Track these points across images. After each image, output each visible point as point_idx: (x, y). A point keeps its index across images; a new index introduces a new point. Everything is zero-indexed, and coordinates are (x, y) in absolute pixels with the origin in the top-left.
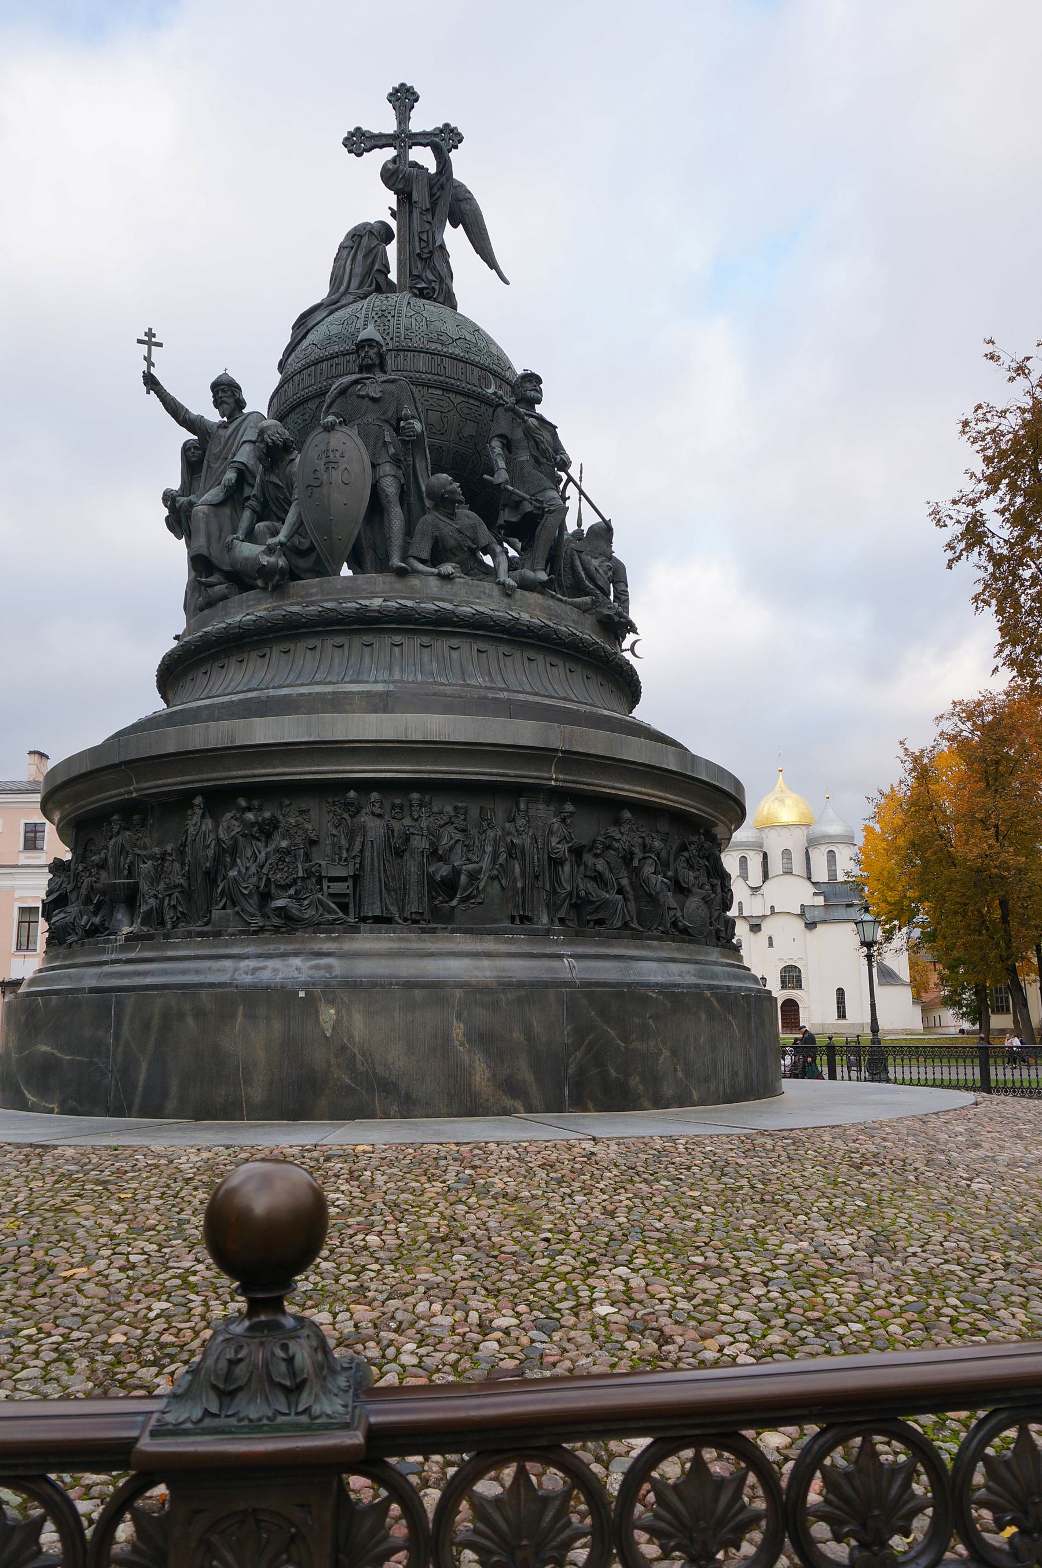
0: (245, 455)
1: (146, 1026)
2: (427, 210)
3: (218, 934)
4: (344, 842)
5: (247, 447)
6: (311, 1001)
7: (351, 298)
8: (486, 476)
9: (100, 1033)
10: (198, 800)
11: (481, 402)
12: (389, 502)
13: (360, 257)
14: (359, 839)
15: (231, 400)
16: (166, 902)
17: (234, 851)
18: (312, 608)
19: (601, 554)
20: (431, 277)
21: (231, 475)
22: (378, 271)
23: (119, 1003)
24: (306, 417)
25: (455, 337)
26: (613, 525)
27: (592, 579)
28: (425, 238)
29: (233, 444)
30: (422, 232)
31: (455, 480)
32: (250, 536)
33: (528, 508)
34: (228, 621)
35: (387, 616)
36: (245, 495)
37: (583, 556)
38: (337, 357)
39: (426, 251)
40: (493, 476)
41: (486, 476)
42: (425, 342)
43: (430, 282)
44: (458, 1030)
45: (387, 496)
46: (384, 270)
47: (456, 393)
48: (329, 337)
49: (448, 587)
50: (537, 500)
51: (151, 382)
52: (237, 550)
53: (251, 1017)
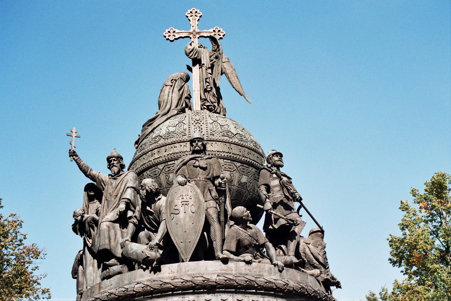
0: (129, 194)
2: (209, 68)
7: (176, 112)
8: (258, 205)
11: (249, 166)
12: (214, 221)
13: (176, 90)
15: (118, 165)
18: (177, 280)
19: (319, 245)
20: (213, 100)
21: (122, 206)
22: (186, 98)
24: (156, 173)
25: (235, 133)
26: (324, 229)
27: (317, 260)
28: (208, 80)
29: (120, 188)
30: (206, 79)
31: (248, 210)
32: (135, 238)
35: (219, 284)
36: (129, 215)
37: (310, 246)
38: (175, 143)
39: (209, 87)
40: (263, 205)
41: (258, 205)
42: (221, 136)
43: (212, 102)
45: (213, 218)
46: (189, 97)
47: (237, 162)
48: (169, 133)
49: (248, 267)
50: (290, 220)
51: (73, 154)
52: (129, 246)
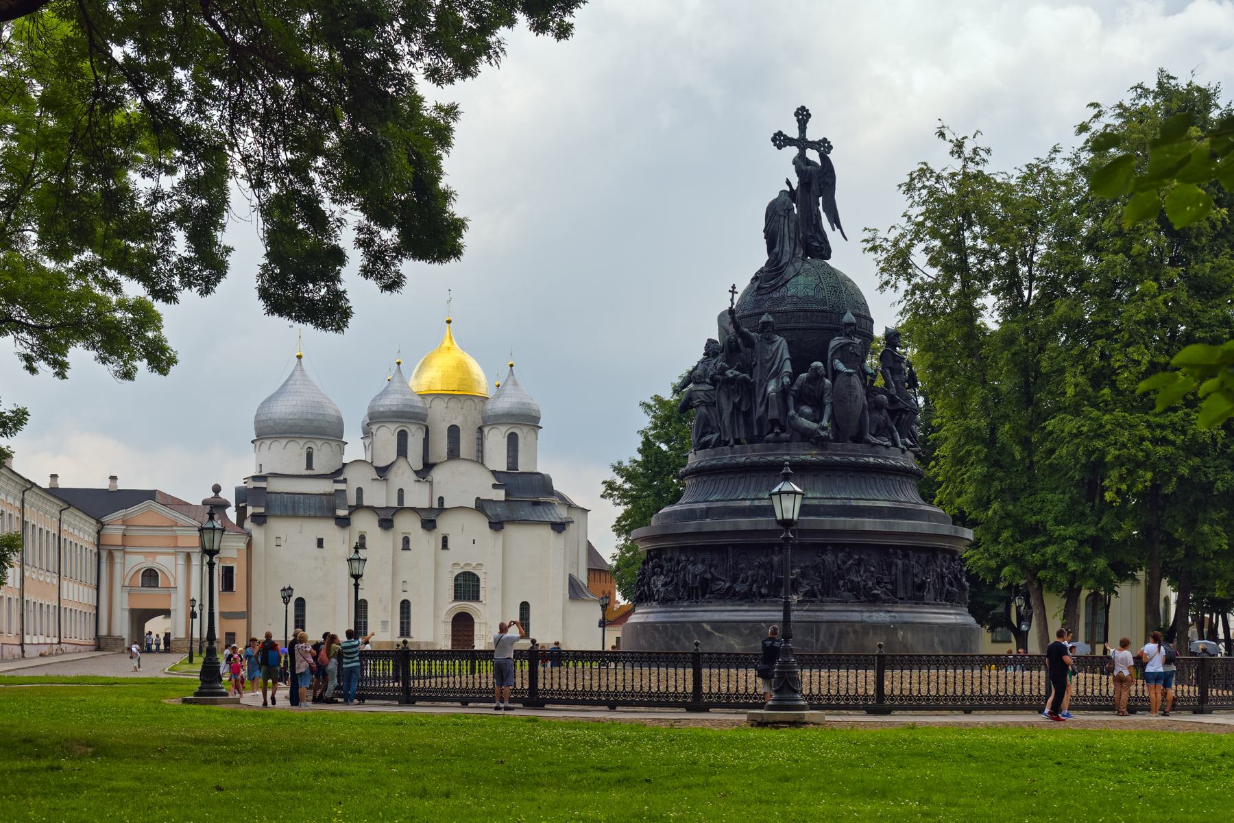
1: (832, 636)
3: (846, 602)
4: (885, 568)
5: (788, 363)
6: (895, 630)
9: (808, 639)
10: (830, 547)
14: (894, 568)
16: (816, 587)
17: (849, 570)
21: (786, 380)
23: (818, 627)
33: (901, 406)
34: (802, 457)
44: (936, 640)
53: (875, 634)
